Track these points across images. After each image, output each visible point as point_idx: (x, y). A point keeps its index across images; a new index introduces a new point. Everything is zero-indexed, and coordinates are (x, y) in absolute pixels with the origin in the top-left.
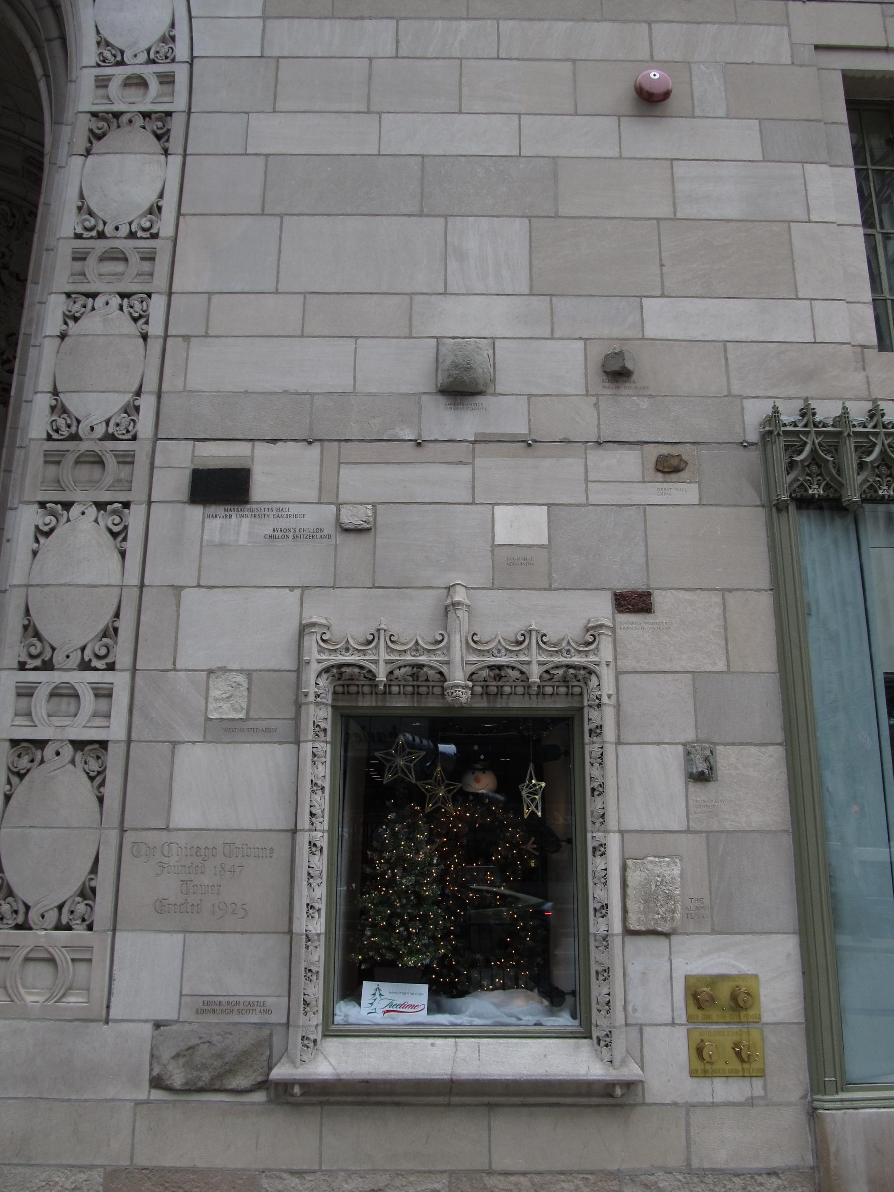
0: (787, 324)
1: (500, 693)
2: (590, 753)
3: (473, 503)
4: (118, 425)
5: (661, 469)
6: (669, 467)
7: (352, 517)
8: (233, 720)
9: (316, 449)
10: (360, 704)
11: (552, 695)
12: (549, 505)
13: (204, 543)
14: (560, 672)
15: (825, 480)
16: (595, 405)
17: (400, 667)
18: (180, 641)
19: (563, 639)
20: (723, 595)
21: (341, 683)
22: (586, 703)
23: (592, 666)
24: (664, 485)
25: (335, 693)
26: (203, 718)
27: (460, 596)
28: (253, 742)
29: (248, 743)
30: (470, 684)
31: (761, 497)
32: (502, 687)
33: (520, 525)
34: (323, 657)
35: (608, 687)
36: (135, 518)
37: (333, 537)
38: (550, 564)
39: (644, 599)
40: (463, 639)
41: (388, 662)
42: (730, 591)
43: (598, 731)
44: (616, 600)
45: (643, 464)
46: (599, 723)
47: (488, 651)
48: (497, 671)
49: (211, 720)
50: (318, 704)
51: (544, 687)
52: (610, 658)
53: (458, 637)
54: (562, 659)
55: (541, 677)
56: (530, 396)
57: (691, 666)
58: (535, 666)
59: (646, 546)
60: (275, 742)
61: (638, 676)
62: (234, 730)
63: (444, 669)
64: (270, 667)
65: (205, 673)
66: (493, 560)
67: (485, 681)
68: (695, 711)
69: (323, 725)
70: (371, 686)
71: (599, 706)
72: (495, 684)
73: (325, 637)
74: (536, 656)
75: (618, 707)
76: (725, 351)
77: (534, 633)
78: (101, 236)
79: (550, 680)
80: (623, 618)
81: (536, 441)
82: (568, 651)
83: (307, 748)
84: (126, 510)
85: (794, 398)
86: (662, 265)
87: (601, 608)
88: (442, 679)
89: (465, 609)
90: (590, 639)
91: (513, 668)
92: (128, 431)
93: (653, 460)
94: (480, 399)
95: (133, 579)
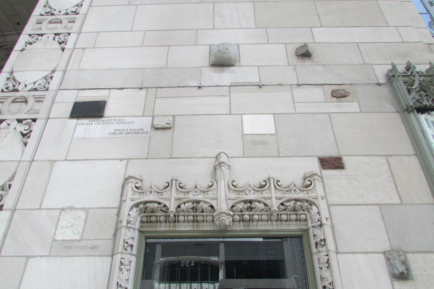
0: (388, 35)
1: (251, 220)
2: (319, 260)
3: (230, 114)
4: (40, 84)
5: (335, 95)
6: (339, 95)
7: (160, 122)
8: (72, 240)
9: (144, 91)
10: (158, 230)
11: (286, 221)
12: (274, 114)
13: (74, 138)
14: (292, 204)
15: (430, 98)
16: (294, 69)
17: (185, 203)
18: (48, 190)
19: (291, 184)
20: (387, 158)
21: (146, 214)
22: (310, 225)
23: (313, 200)
24: (338, 103)
25: (142, 222)
26: (51, 240)
27: (223, 158)
28: (82, 256)
29: (79, 256)
30: (232, 213)
31: (395, 108)
32: (253, 215)
33: (259, 124)
34: (135, 197)
35: (325, 214)
36: (36, 128)
37: (149, 133)
38: (278, 144)
39: (338, 161)
40: (226, 184)
41: (176, 199)
42: (391, 156)
43: (323, 243)
44: (320, 162)
45: (324, 94)
46: (322, 238)
47: (242, 191)
48: (249, 204)
49: (56, 241)
50: (128, 228)
51: (281, 215)
52: (323, 195)
53: (223, 182)
54: (291, 195)
55: (278, 208)
56: (259, 67)
57: (377, 200)
58: (274, 200)
59: (334, 133)
60: (97, 256)
61: (342, 207)
62: (69, 247)
63: (214, 203)
64: (101, 206)
65: (58, 211)
66: (243, 142)
67: (241, 211)
68: (386, 230)
69: (130, 242)
70: (165, 216)
71: (321, 225)
72: (247, 213)
73: (137, 185)
74: (274, 194)
75: (333, 227)
76: (358, 46)
77: (272, 180)
78: (53, 14)
79: (285, 210)
80: (328, 173)
81: (264, 85)
82: (295, 190)
83: (118, 258)
84: (34, 123)
85: (400, 64)
86: (319, 16)
87: (314, 166)
88: (213, 210)
89: (227, 166)
90: (309, 183)
91: (259, 202)
92: (45, 87)
93: (330, 92)
94: (232, 68)
95: (27, 157)
